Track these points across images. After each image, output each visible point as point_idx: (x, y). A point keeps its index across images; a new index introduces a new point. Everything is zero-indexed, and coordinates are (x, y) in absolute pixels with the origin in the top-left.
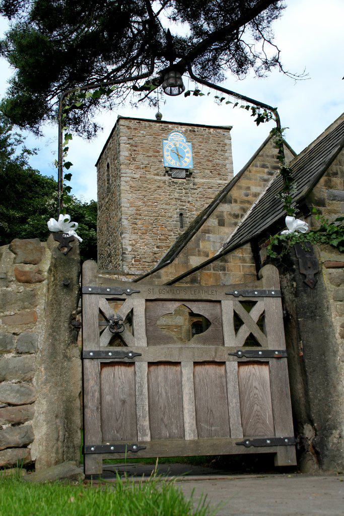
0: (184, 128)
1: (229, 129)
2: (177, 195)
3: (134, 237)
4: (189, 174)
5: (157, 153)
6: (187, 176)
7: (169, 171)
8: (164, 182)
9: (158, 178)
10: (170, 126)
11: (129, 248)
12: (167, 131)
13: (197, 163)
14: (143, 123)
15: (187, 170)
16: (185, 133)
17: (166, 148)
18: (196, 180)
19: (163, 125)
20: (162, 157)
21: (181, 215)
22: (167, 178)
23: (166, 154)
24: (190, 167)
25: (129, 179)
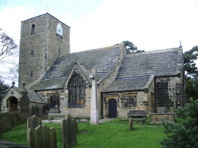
0: (61, 23)
1: (70, 28)
2: (59, 43)
3: (49, 52)
4: (61, 38)
5: (55, 28)
6: (61, 38)
7: (57, 35)
8: (56, 38)
9: (55, 36)
10: (58, 21)
11: (48, 56)
12: (58, 23)
13: (63, 35)
14: (53, 17)
15: (61, 36)
16: (61, 25)
17: (57, 28)
18: (63, 40)
19: (57, 20)
20: (56, 30)
21: (59, 49)
22: (57, 37)
23: (57, 29)
24: (62, 36)
25: (48, 34)
